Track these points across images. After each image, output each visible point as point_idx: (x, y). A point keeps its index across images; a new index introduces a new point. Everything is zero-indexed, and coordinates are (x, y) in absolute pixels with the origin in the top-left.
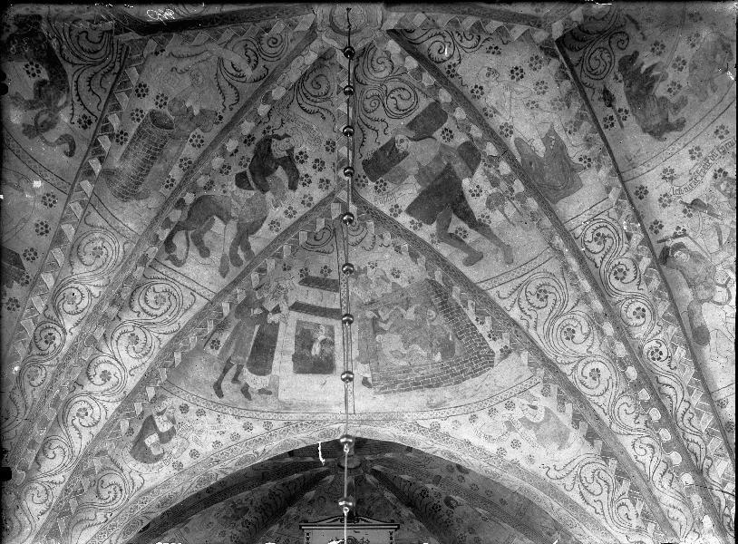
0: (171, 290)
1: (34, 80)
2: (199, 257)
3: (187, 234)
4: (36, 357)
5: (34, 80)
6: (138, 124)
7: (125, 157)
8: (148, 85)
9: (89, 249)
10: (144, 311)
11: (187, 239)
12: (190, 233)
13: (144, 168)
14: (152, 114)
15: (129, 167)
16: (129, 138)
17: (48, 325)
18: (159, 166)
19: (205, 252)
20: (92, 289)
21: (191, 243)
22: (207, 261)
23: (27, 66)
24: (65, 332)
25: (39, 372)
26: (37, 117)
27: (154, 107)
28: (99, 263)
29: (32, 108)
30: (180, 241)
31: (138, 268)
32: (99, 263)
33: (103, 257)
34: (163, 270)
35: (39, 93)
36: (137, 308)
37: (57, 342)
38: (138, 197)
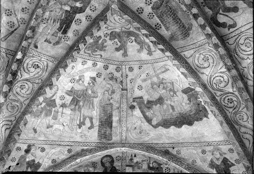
0: (246, 37)
1: (134, 42)
2: (237, 14)
3: (221, 14)
4: (234, 111)
5: (134, 42)
6: (155, 17)
7: (167, 29)
8: (138, 7)
9: (202, 62)
10: (249, 55)
11: (224, 15)
12: (221, 12)
13: (176, 20)
14: (153, 8)
15: (174, 28)
16: (160, 23)
17: (223, 98)
18: (180, 14)
19: (235, 9)
20: (221, 70)
21: (226, 14)
22: (241, 11)
23: (129, 42)
24: (233, 93)
25: (242, 114)
26: (146, 49)
27: (150, 6)
28: (211, 61)
29: (143, 48)
30: (222, 19)
31: (219, 50)
32: (211, 61)
33: (210, 57)
34: (234, 34)
35: (139, 43)
36: (246, 57)
37: (234, 99)
38: (190, 29)
